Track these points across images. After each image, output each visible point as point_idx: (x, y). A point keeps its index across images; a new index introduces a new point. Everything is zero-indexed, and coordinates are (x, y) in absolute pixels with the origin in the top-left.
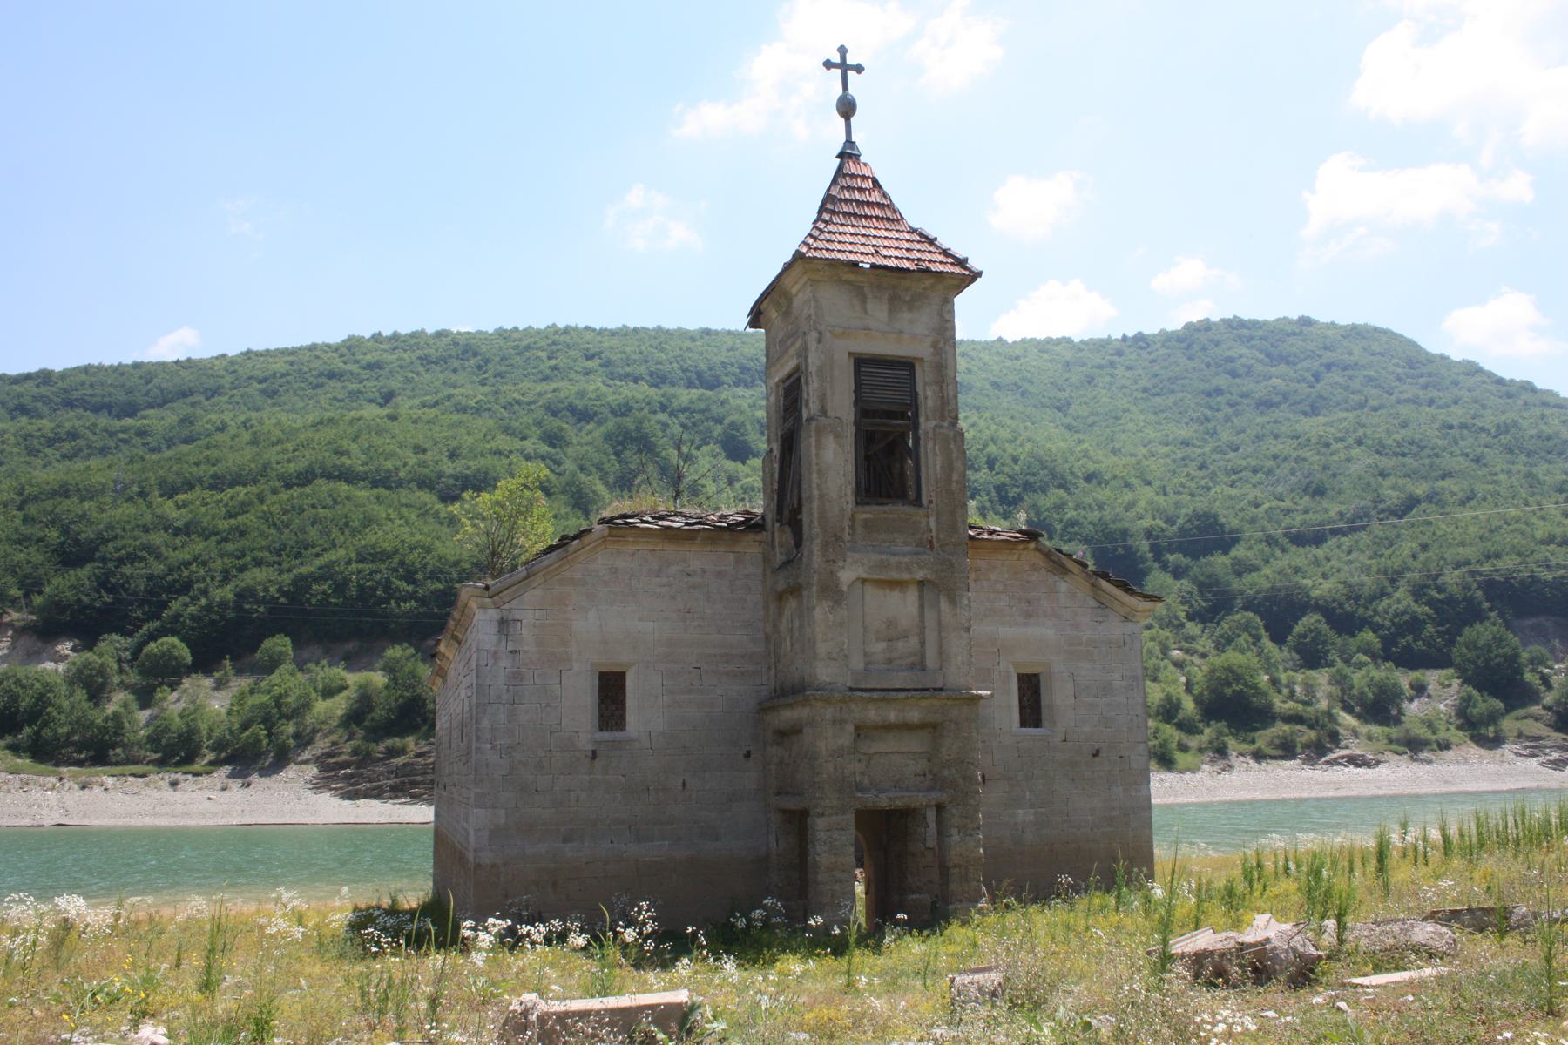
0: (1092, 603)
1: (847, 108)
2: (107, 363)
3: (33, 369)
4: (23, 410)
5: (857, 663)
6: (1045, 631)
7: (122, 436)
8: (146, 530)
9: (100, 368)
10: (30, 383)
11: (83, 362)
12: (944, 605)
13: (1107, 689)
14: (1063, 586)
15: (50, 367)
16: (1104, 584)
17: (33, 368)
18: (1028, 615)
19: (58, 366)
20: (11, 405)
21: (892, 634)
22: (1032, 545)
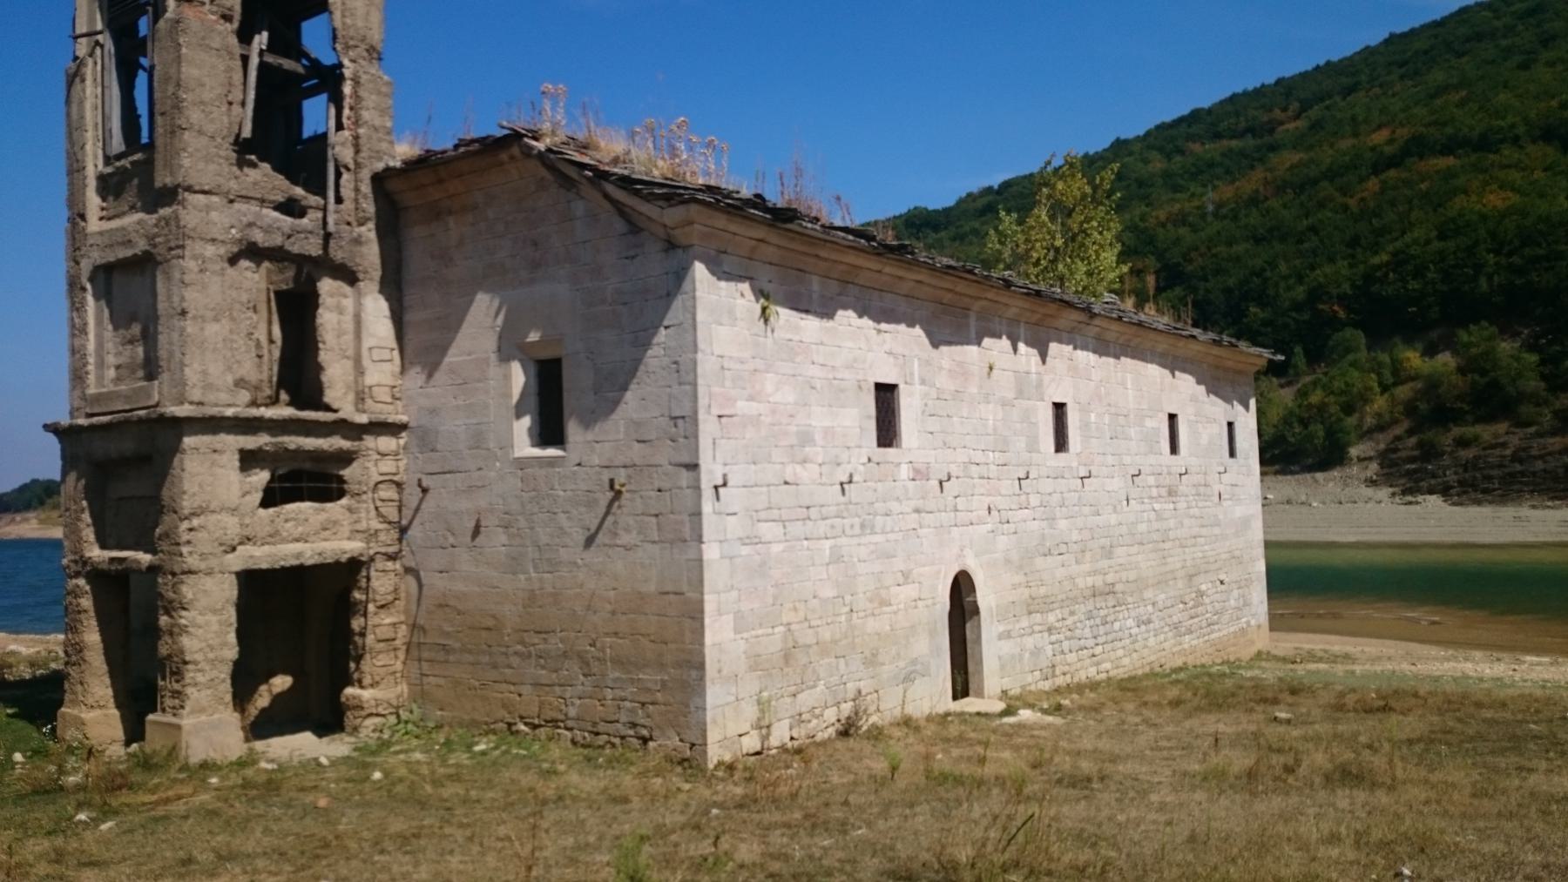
0: (620, 226)
2: (1250, 88)
3: (1186, 111)
10: (1184, 125)
11: (1227, 94)
14: (579, 208)
16: (610, 188)
17: (1185, 111)
19: (1206, 103)
22: (515, 150)
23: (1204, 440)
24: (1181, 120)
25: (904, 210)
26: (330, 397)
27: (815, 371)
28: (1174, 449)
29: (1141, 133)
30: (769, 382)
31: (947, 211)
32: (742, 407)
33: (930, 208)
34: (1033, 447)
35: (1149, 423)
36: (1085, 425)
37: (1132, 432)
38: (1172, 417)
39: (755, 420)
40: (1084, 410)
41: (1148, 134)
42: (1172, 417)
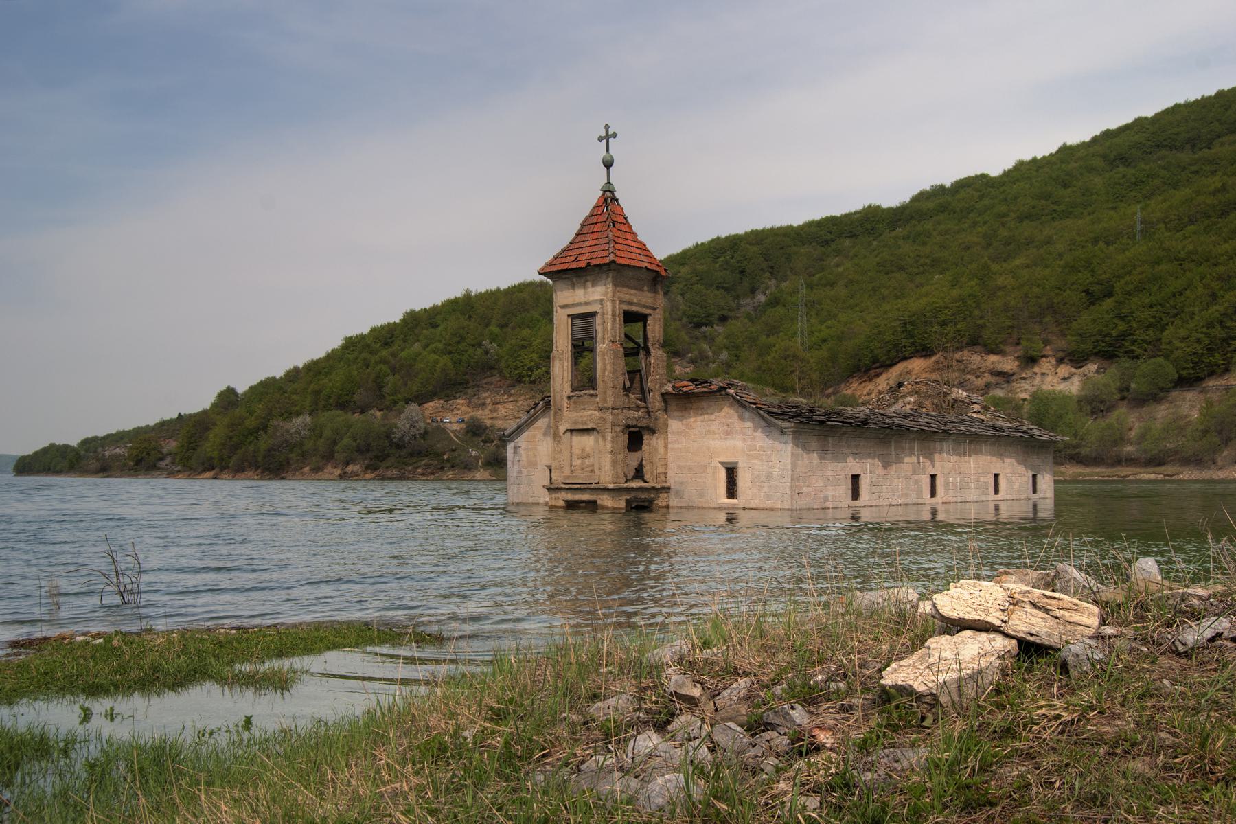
1: (608, 164)
2: (1192, 99)
3: (1130, 120)
4: (1123, 159)
5: (567, 472)
6: (737, 443)
7: (1193, 168)
8: (1157, 262)
9: (1188, 105)
11: (1170, 104)
12: (600, 440)
13: (769, 476)
15: (1144, 115)
18: (727, 433)
20: (1112, 156)
21: (584, 456)
23: (1016, 485)
24: (1126, 128)
25: (860, 208)
26: (646, 477)
27: (830, 473)
28: (997, 491)
29: (1087, 139)
30: (814, 480)
31: (903, 208)
32: (805, 489)
33: (885, 206)
34: (919, 494)
35: (982, 480)
36: (947, 485)
37: (972, 485)
38: (996, 476)
39: (809, 493)
40: (947, 477)
41: (1095, 140)
42: (996, 476)
